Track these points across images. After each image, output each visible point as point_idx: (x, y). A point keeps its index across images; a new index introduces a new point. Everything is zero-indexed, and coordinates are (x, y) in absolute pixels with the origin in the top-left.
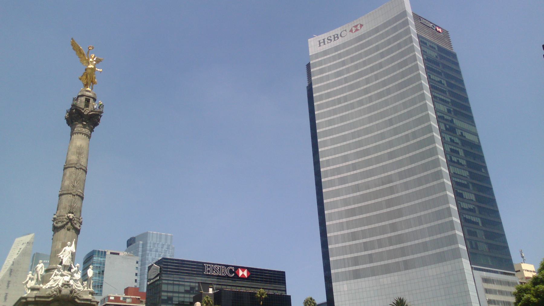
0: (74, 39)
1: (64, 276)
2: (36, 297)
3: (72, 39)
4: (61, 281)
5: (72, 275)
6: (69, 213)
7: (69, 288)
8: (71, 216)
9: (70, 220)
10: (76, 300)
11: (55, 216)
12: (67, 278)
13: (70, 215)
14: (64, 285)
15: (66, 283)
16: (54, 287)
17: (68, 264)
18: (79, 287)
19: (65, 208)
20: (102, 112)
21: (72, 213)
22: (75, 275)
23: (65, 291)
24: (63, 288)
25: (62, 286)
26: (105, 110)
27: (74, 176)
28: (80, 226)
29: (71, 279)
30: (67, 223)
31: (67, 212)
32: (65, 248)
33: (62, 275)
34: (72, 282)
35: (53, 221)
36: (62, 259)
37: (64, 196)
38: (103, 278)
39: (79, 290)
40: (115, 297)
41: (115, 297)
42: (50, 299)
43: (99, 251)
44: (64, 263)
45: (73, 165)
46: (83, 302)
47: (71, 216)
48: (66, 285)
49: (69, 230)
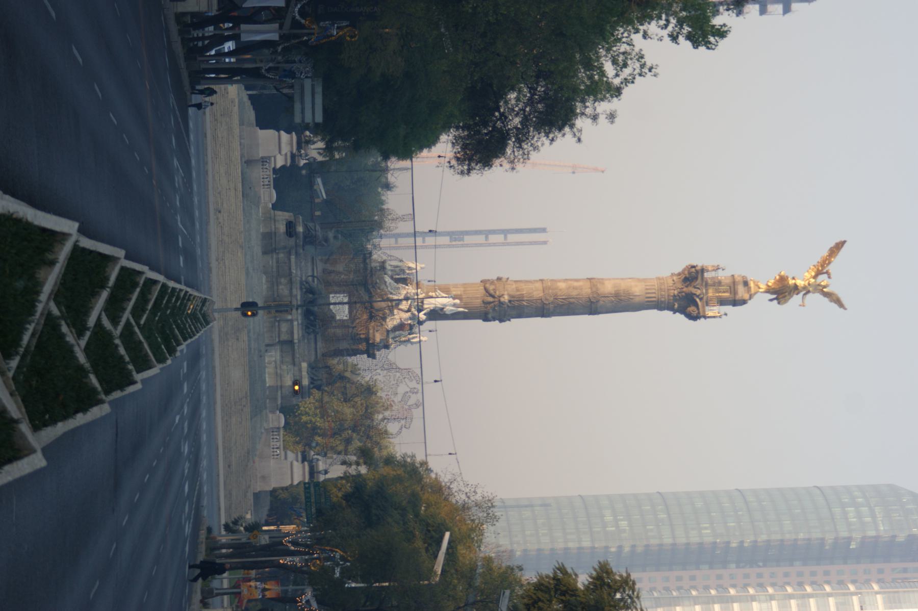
0: (845, 245)
3: (844, 242)
11: (504, 280)
17: (425, 306)
18: (391, 323)
19: (518, 290)
21: (510, 301)
28: (494, 319)
30: (493, 297)
31: (512, 293)
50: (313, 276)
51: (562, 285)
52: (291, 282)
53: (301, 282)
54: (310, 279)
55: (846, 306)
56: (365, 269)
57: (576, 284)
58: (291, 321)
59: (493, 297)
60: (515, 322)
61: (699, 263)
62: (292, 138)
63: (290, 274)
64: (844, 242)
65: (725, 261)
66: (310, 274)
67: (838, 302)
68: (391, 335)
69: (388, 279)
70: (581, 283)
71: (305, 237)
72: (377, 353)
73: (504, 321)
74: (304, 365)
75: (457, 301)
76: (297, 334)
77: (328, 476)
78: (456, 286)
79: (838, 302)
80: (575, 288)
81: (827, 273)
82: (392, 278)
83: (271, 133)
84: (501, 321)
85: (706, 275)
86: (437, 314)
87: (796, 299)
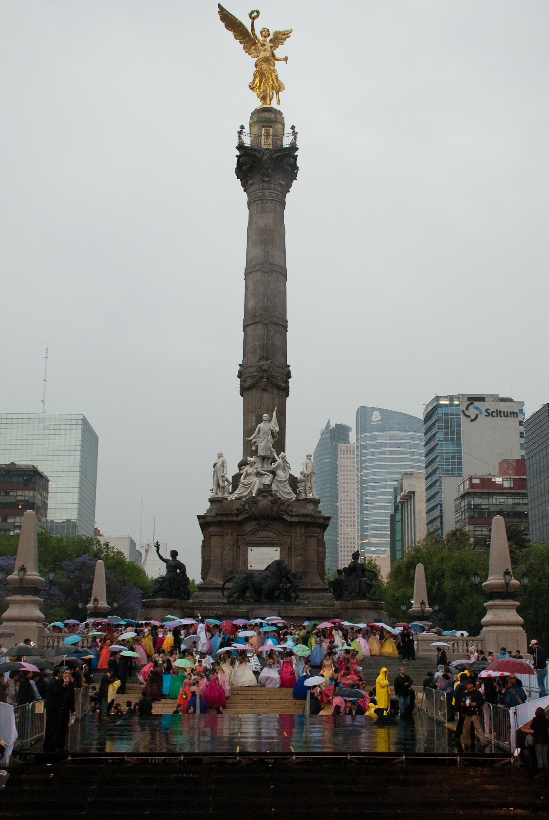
1: (262, 475)
2: (217, 515)
3: (220, 6)
4: (256, 483)
5: (274, 473)
7: (270, 498)
9: (265, 371)
10: (286, 517)
12: (267, 480)
13: (262, 363)
14: (260, 492)
15: (267, 488)
16: (245, 496)
17: (268, 454)
18: (286, 493)
19: (254, 351)
20: (294, 148)
21: (267, 359)
23: (264, 502)
24: (260, 498)
25: (257, 494)
26: (299, 145)
29: (272, 482)
31: (257, 358)
32: (259, 425)
33: (259, 474)
34: (274, 487)
35: (239, 377)
36: (257, 446)
37: (249, 329)
38: (459, 445)
39: (289, 499)
42: (241, 518)
44: (261, 453)
45: (257, 268)
46: (297, 519)
47: (265, 364)
48: (266, 491)
49: (264, 390)
50: (223, 589)
51: (251, 303)
53: (230, 603)
54: (226, 593)
55: (289, 29)
56: (220, 524)
59: (262, 377)
60: (293, 359)
62: (14, 602)
64: (220, 6)
66: (221, 594)
68: (303, 496)
70: (250, 283)
71: (170, 595)
73: (289, 372)
78: (245, 423)
81: (254, 15)
82: (231, 493)
86: (279, 442)
87: (279, 66)
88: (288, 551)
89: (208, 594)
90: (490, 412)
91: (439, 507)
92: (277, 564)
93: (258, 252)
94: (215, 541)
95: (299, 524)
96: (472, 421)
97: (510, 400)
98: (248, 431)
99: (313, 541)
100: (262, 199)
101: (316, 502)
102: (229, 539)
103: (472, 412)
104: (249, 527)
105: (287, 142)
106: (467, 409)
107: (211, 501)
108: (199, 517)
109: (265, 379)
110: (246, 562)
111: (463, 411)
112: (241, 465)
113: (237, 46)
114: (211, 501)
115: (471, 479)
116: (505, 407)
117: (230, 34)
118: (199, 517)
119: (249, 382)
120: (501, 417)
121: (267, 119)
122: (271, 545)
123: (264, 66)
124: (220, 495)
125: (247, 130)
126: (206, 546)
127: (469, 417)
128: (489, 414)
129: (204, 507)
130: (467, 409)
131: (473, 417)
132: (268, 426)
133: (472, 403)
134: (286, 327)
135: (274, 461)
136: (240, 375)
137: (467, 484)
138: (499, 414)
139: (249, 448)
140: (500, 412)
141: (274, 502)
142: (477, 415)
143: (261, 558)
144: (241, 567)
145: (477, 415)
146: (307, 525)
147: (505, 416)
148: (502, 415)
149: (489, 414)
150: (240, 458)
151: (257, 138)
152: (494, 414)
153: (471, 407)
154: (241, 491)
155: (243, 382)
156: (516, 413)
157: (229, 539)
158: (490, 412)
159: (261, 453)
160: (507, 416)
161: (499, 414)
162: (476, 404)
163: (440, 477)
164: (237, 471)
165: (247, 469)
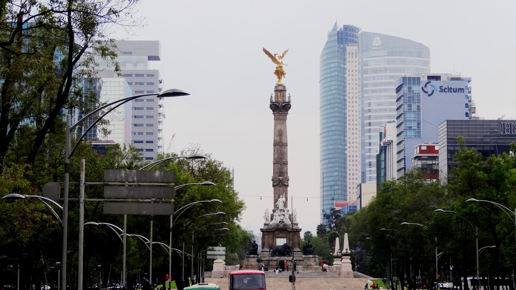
6: (280, 176)
8: (281, 178)
12: (282, 217)
14: (280, 222)
18: (288, 222)
19: (277, 173)
22: (286, 215)
23: (281, 225)
27: (279, 151)
34: (284, 220)
37: (275, 165)
40: (428, 147)
41: (428, 147)
43: (409, 78)
44: (280, 208)
47: (281, 178)
48: (281, 222)
50: (269, 252)
51: (276, 156)
52: (271, 260)
53: (271, 256)
56: (268, 232)
57: (276, 151)
58: (287, 260)
61: (269, 103)
63: (268, 260)
65: (268, 94)
67: (286, 52)
69: (271, 223)
72: (300, 228)
74: (304, 256)
75: (281, 196)
76: (291, 258)
77: (348, 249)
78: (275, 197)
79: (286, 52)
80: (277, 151)
81: (275, 55)
83: (215, 266)
84: (288, 180)
85: (274, 101)
88: (289, 240)
89: (265, 253)
90: (443, 88)
91: (403, 161)
92: (285, 245)
93: (278, 138)
94: (266, 237)
95: (291, 231)
96: (429, 95)
97: (459, 79)
98: (276, 201)
99: (296, 237)
100: (279, 119)
101: (297, 224)
102: (271, 236)
103: (429, 89)
104: (276, 233)
105: (287, 101)
106: (426, 86)
107: (265, 225)
108: (261, 229)
109: (280, 183)
110: (276, 243)
111: (423, 88)
112: (274, 211)
113: (270, 59)
114: (265, 225)
115: (420, 147)
116: (455, 85)
117: (267, 56)
118: (261, 229)
119: (275, 184)
120: (451, 92)
121: (280, 90)
122: (283, 238)
123: (279, 69)
124: (267, 223)
125: (274, 96)
126: (263, 238)
127: (427, 92)
128: (442, 90)
129: (262, 227)
130: (426, 86)
131: (430, 93)
132: (282, 200)
133: (429, 82)
134: (287, 164)
135: (284, 211)
136: (273, 180)
137: (418, 148)
138: (450, 90)
139: (276, 207)
140: (451, 88)
141: (284, 225)
142: (433, 91)
143: (281, 242)
144: (274, 245)
145: (433, 91)
146: (295, 232)
147: (454, 92)
148: (452, 91)
149: (442, 90)
150: (273, 208)
151: (277, 97)
152: (446, 90)
153: (428, 85)
154: (274, 221)
155: (274, 183)
156: (463, 89)
157: (271, 236)
158: (443, 88)
159: (280, 208)
160: (456, 92)
161: (450, 90)
162: (433, 82)
163: (404, 138)
164: (272, 212)
165: (275, 214)
